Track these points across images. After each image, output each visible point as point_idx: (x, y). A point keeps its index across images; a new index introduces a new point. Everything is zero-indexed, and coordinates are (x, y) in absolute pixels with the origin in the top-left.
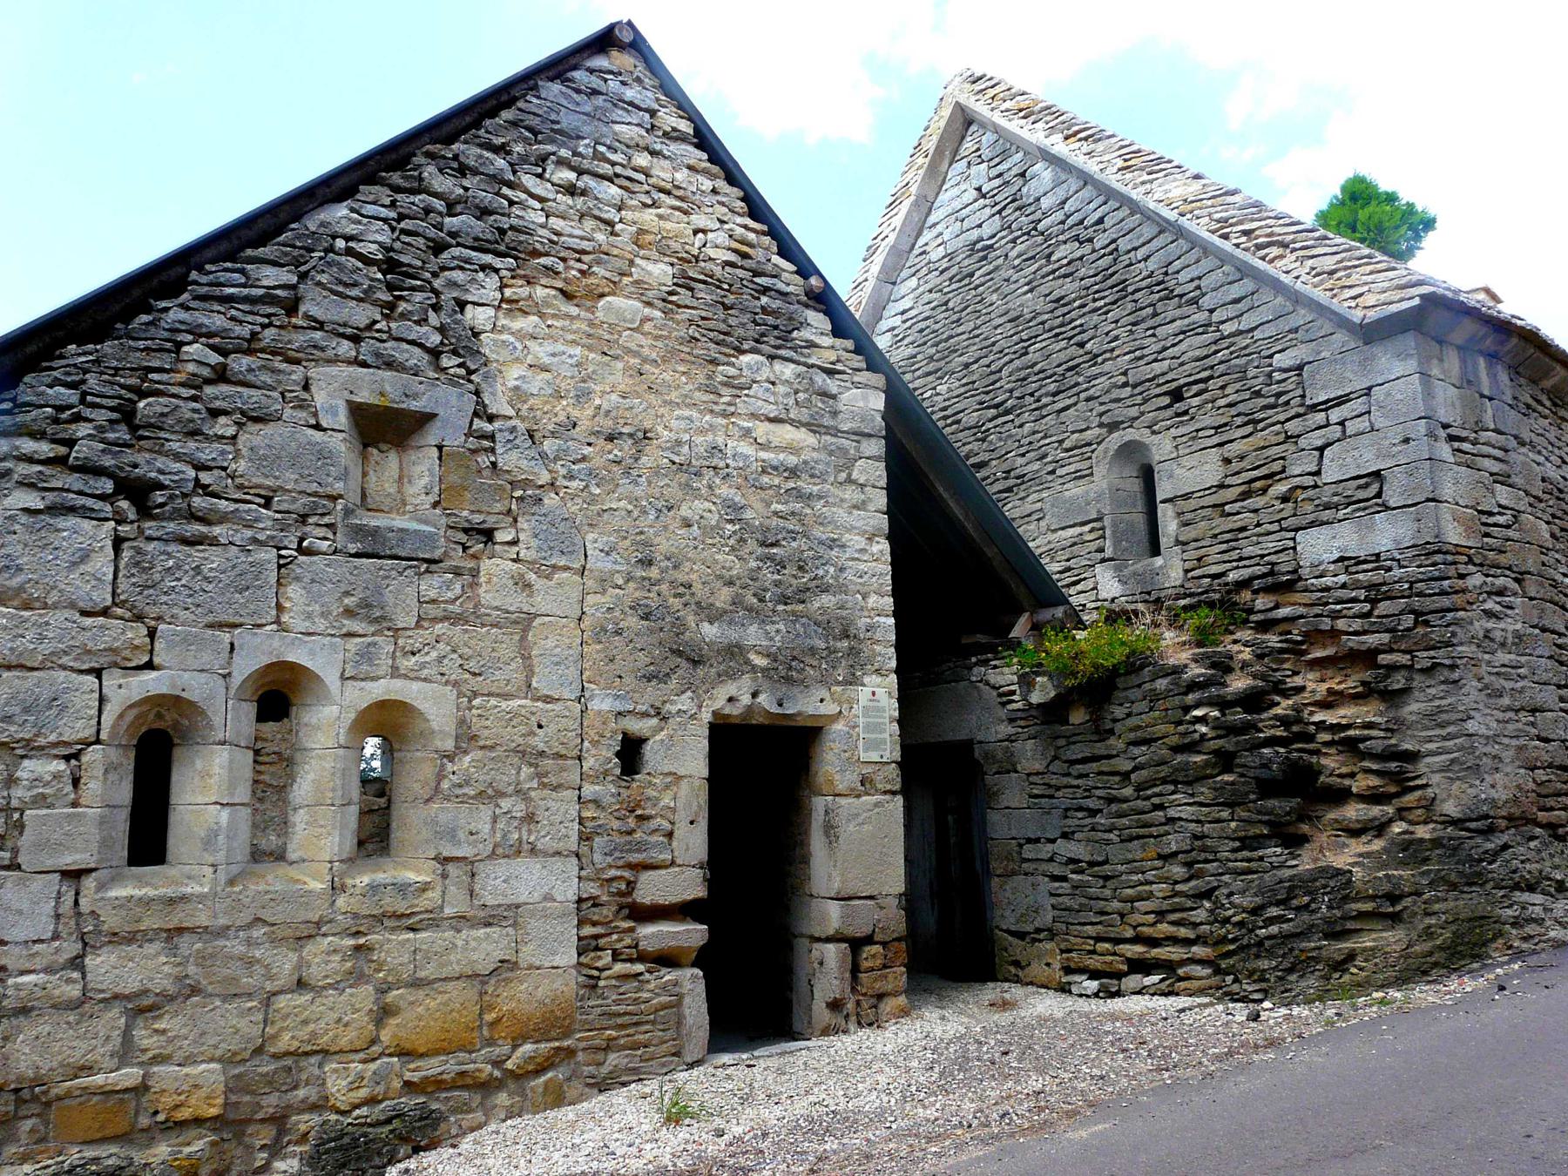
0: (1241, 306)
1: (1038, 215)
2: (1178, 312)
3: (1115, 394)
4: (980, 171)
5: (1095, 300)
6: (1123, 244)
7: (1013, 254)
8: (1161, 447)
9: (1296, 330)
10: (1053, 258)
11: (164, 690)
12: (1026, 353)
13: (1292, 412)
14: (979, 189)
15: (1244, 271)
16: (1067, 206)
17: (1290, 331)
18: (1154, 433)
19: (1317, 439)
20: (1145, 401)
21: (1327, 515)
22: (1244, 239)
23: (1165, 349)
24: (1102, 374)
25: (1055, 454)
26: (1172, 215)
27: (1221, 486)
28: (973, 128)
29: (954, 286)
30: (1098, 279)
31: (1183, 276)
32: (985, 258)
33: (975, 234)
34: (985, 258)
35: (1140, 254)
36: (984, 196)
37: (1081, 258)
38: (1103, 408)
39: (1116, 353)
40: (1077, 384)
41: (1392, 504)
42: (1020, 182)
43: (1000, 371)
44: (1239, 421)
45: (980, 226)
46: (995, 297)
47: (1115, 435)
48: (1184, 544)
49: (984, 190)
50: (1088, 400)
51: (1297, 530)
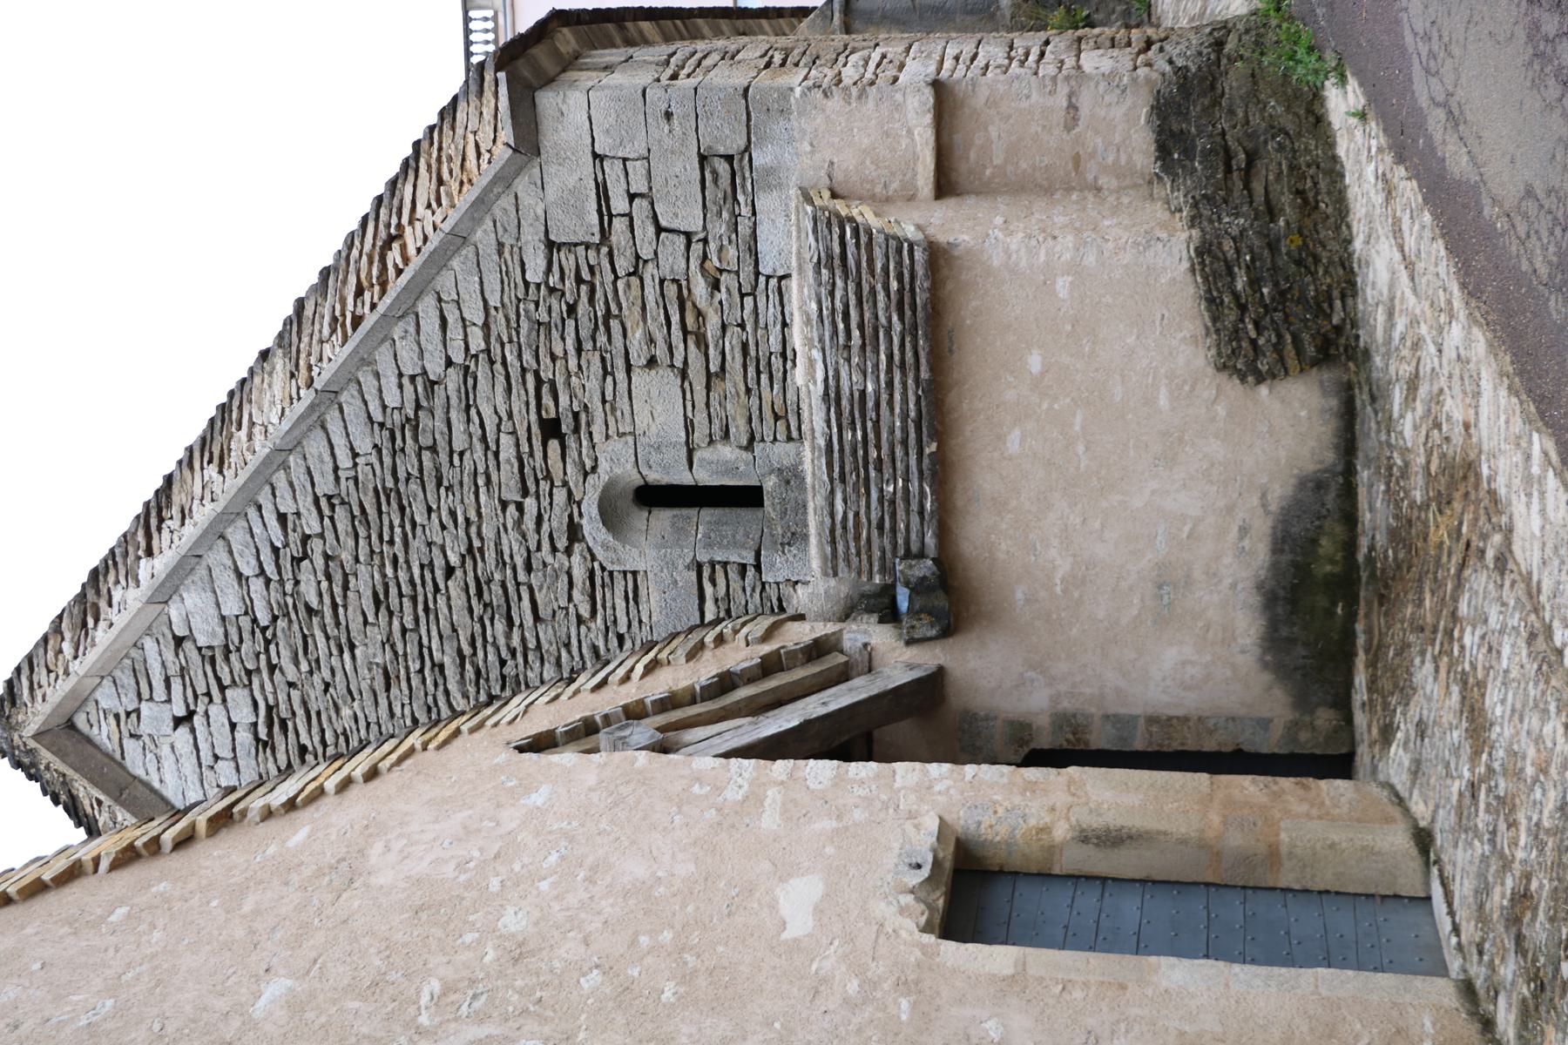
0: (453, 316)
1: (245, 623)
2: (439, 413)
3: (529, 523)
4: (155, 717)
5: (391, 542)
6: (325, 486)
7: (291, 673)
8: (617, 463)
9: (500, 245)
10: (314, 604)
12: (442, 667)
13: (605, 263)
14: (178, 722)
15: (407, 310)
17: (500, 253)
18: (594, 469)
19: (645, 231)
20: (548, 476)
21: (744, 228)
22: (367, 295)
23: (484, 439)
24: (498, 544)
25: (595, 633)
26: (307, 396)
27: (684, 374)
28: (80, 721)
30: (362, 532)
31: (392, 399)
32: (283, 723)
33: (244, 736)
34: (283, 723)
35: (345, 461)
36: (191, 714)
37: (327, 557)
38: (546, 545)
39: (473, 516)
40: (503, 585)
41: (742, 143)
42: (188, 645)
44: (602, 339)
45: (233, 726)
46: (346, 712)
48: (752, 439)
50: (529, 568)
51: (757, 274)
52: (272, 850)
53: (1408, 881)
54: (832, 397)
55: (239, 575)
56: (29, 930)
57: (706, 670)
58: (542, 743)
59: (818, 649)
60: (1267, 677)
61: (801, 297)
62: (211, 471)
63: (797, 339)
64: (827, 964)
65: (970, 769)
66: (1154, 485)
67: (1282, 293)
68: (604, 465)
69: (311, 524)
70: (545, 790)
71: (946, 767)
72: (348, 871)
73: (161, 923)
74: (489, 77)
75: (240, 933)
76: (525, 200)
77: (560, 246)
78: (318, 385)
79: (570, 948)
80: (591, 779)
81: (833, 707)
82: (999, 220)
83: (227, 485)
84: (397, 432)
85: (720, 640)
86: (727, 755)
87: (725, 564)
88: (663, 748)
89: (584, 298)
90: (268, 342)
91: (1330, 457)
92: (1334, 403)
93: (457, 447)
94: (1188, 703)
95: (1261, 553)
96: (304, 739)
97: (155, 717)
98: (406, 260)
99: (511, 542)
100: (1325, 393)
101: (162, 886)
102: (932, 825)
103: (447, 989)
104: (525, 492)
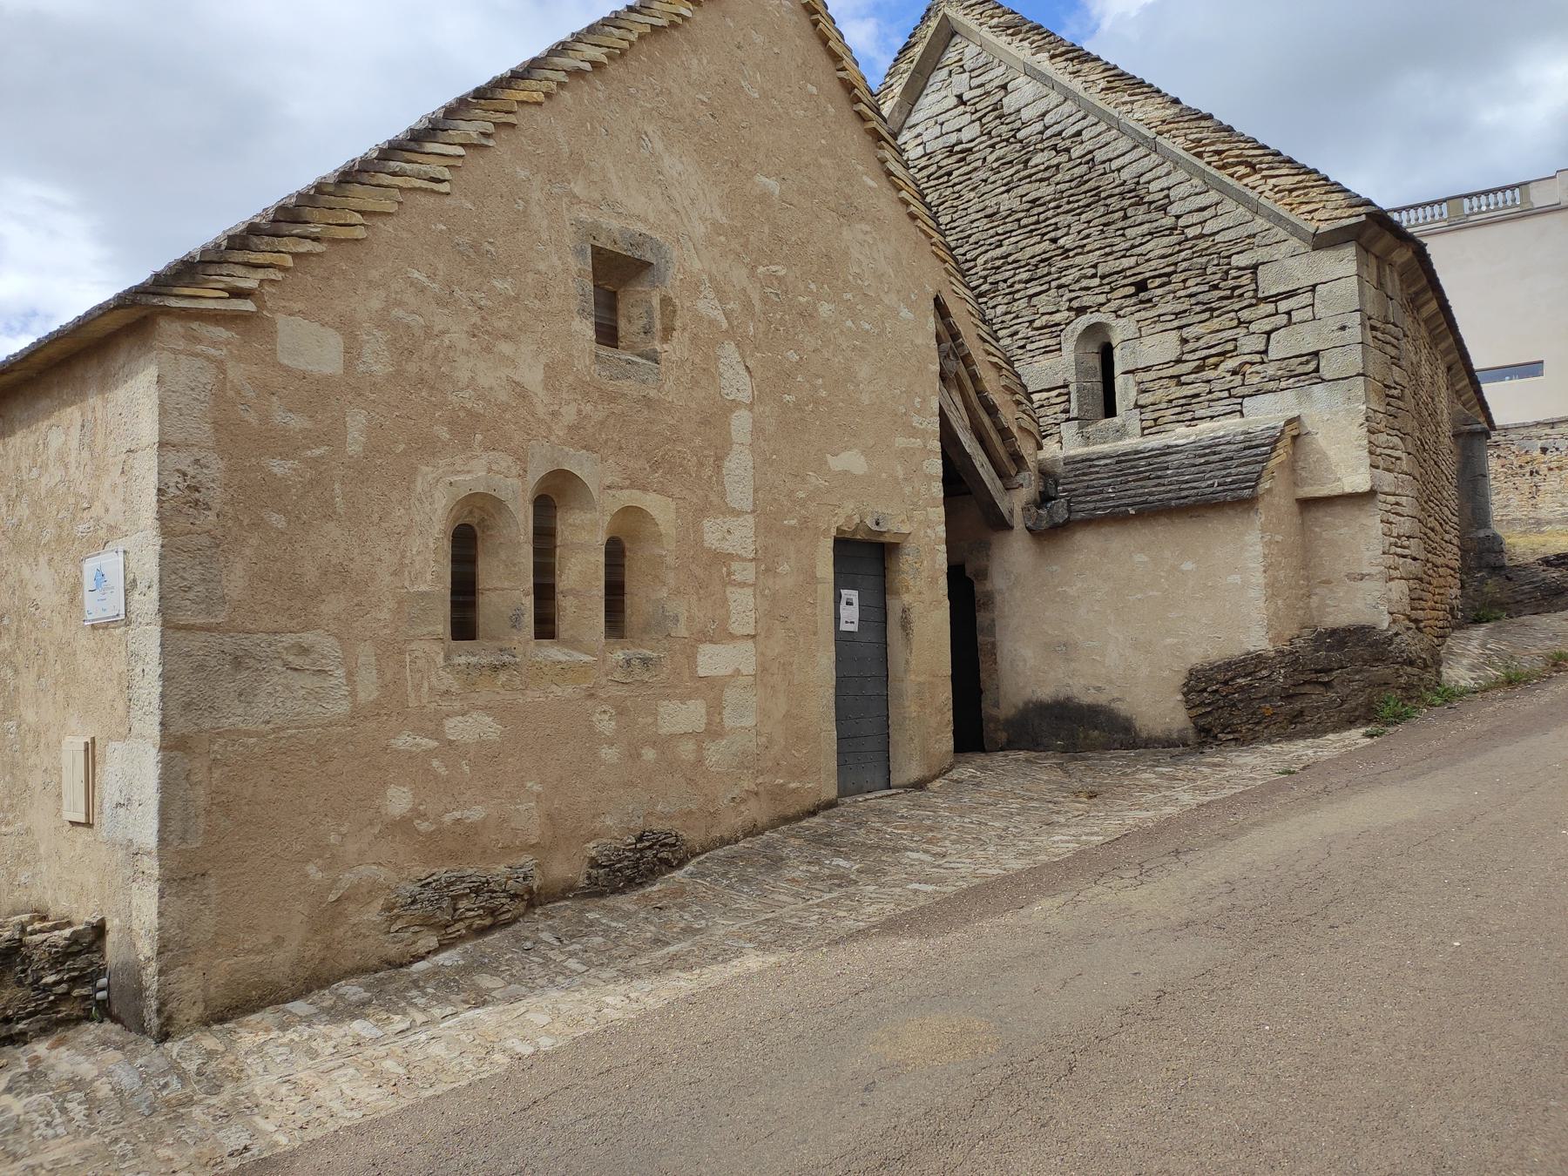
0: (1206, 214)
1: (1018, 124)
2: (1147, 217)
3: (1085, 283)
4: (961, 83)
5: (1069, 203)
6: (1100, 156)
9: (1254, 236)
10: (1031, 164)
13: (1246, 303)
14: (960, 97)
16: (1047, 119)
17: (1248, 237)
18: (1118, 316)
19: (1266, 325)
20: (1112, 290)
22: (1216, 158)
23: (1133, 247)
25: (1024, 331)
26: (1151, 134)
27: (1179, 361)
28: (957, 39)
29: (932, 183)
30: (1073, 184)
31: (1154, 186)
33: (953, 138)
34: (964, 159)
35: (1115, 164)
36: (964, 103)
37: (1057, 166)
38: (1073, 295)
40: (1049, 273)
41: (1326, 377)
42: (1002, 93)
44: (1198, 308)
45: (959, 130)
46: (972, 194)
47: (1084, 317)
48: (1142, 407)
50: (1059, 287)
52: (860, 168)
53: (896, 779)
54: (1167, 451)
55: (1044, 115)
56: (798, 41)
57: (997, 397)
58: (940, 307)
59: (1018, 459)
60: (1021, 705)
61: (1229, 426)
62: (1103, 84)
63: (1204, 426)
64: (813, 480)
65: (943, 547)
66: (1121, 638)
67: (1234, 705)
68: (1122, 321)
69: (1076, 153)
70: (911, 316)
71: (944, 535)
72: (848, 213)
73: (809, 114)
74: (1361, 210)
75: (805, 159)
76: (1283, 247)
77: (1255, 273)
78: (1159, 139)
79: (810, 342)
80: (919, 341)
81: (980, 470)
82: (1279, 538)
83: (1094, 97)
84: (1135, 194)
85: (1019, 403)
86: (942, 415)
87: (1069, 401)
88: (943, 377)
89: (1223, 293)
90: (1185, 102)
91: (1144, 735)
92: (1175, 736)
93: (1128, 232)
94: (1004, 664)
95: (1087, 699)
96: (956, 173)
97: (961, 83)
98: (1240, 178)
99: (1074, 273)
100: (1180, 731)
101: (831, 110)
102: (905, 529)
103: (780, 280)
104: (1103, 277)
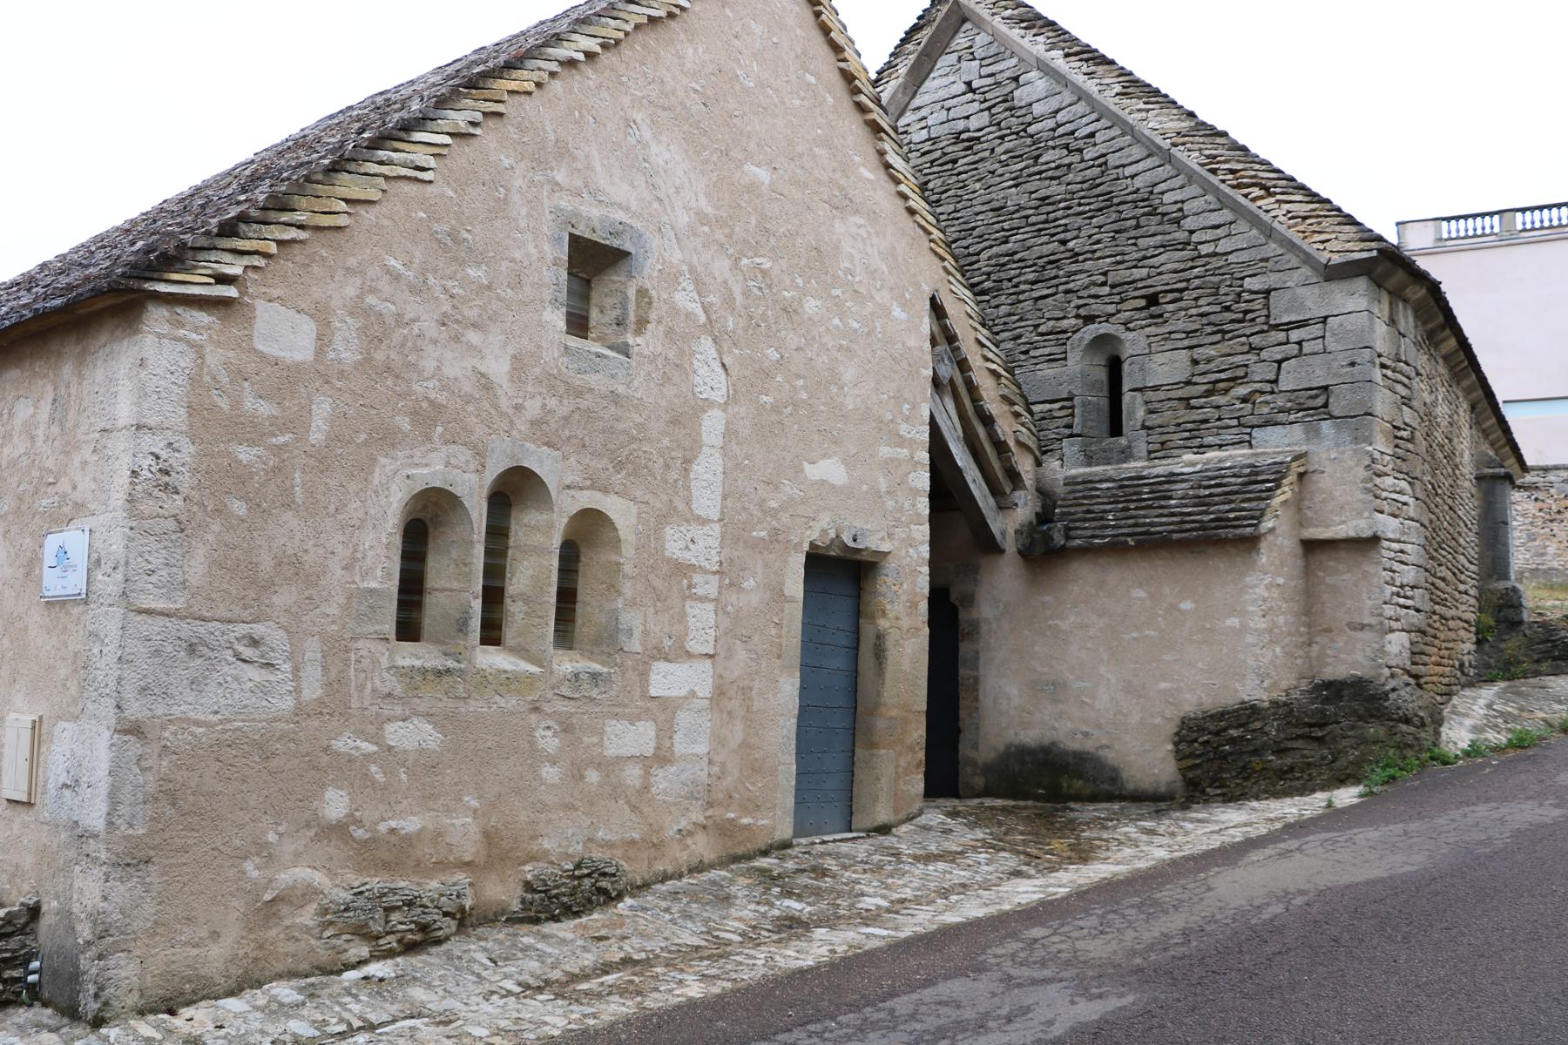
1: (1029, 118)
2: (1160, 228)
3: (1093, 290)
4: (971, 70)
5: (1080, 205)
6: (1113, 160)
7: (999, 150)
8: (1133, 343)
9: (1267, 260)
10: (1041, 160)
11: (438, 484)
12: (1007, 242)
14: (969, 84)
15: (1224, 203)
16: (1059, 116)
17: (1262, 260)
18: (1128, 329)
20: (1123, 301)
21: (1281, 417)
23: (1145, 258)
24: (1081, 272)
26: (1166, 144)
27: (1188, 383)
28: (967, 26)
29: (935, 169)
30: (1085, 186)
31: (1167, 198)
32: (969, 148)
33: (961, 125)
34: (969, 148)
35: (1128, 171)
36: (973, 91)
37: (1069, 165)
38: (1081, 302)
39: (1097, 255)
41: (1336, 413)
42: (1014, 85)
43: (978, 254)
44: (1209, 329)
45: (967, 118)
46: (978, 185)
47: (1091, 327)
48: (1149, 428)
49: (974, 85)
50: (1067, 292)
51: (1253, 427)
52: (857, 159)
53: (860, 821)
54: (1172, 478)
55: (1057, 112)
56: (798, 31)
57: (993, 407)
58: (937, 309)
59: (1014, 477)
60: (1002, 748)
61: (1240, 454)
62: (1118, 88)
63: (1212, 454)
64: (788, 489)
65: (926, 569)
66: (1113, 680)
67: (1225, 758)
68: (1131, 335)
69: (1089, 154)
70: (903, 316)
71: (927, 556)
72: (843, 205)
73: (806, 103)
74: (1373, 245)
75: (799, 149)
76: (1296, 275)
77: (1267, 298)
78: (1174, 150)
79: (793, 340)
80: (911, 343)
81: (972, 486)
82: (1280, 581)
83: (1109, 100)
84: (1148, 202)
85: (1017, 415)
86: (933, 422)
87: (1072, 415)
88: (936, 382)
89: (1234, 316)
90: (1202, 117)
91: (1131, 786)
92: (1163, 789)
93: (1141, 242)
94: (986, 702)
95: (1074, 745)
96: (961, 162)
97: (971, 70)
98: (1254, 200)
99: (1082, 280)
100: (1168, 784)
101: (830, 100)
102: (885, 547)
103: (764, 273)
104: (1112, 287)
